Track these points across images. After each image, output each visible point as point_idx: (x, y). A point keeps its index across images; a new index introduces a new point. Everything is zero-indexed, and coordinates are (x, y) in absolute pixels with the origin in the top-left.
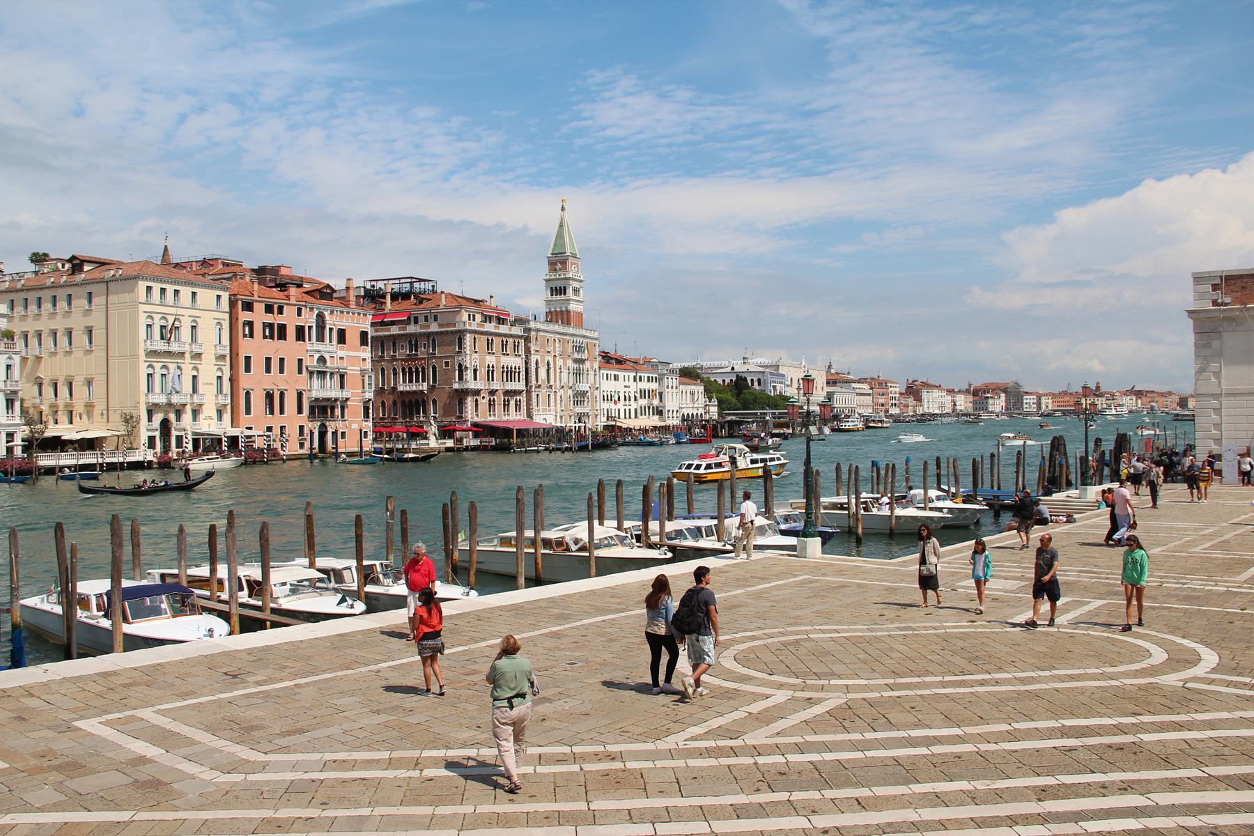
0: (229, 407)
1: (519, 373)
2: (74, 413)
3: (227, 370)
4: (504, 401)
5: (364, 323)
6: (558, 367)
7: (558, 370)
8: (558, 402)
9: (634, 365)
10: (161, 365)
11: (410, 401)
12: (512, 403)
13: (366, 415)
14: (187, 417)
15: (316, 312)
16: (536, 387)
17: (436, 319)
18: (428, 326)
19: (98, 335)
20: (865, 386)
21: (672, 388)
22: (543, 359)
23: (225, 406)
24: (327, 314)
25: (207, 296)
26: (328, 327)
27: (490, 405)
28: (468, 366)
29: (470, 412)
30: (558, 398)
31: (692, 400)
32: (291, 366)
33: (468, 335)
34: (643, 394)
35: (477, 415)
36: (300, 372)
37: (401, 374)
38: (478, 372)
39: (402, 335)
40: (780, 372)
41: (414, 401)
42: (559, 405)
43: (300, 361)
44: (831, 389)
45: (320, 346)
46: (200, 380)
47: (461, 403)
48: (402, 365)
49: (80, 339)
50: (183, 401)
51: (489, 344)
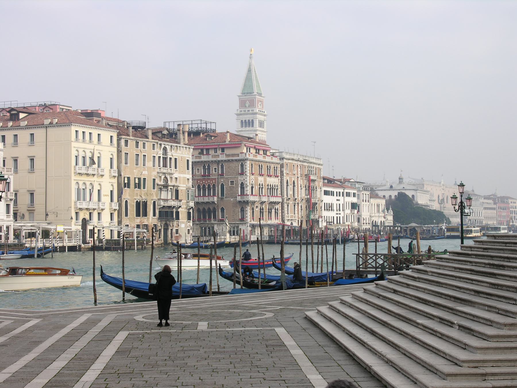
0: (116, 212)
1: (277, 189)
2: (18, 214)
3: (116, 186)
5: (188, 154)
6: (299, 185)
7: (300, 188)
8: (300, 210)
9: (342, 183)
10: (82, 182)
11: (204, 209)
12: (273, 211)
13: (189, 218)
15: (163, 146)
16: (287, 200)
18: (218, 156)
19: (39, 164)
20: (491, 201)
21: (366, 201)
23: (115, 210)
25: (106, 135)
26: (169, 157)
27: (260, 212)
28: (248, 184)
29: (249, 217)
30: (300, 208)
33: (248, 162)
35: (253, 219)
36: (154, 188)
38: (254, 189)
39: (198, 162)
40: (425, 189)
41: (206, 208)
42: (300, 213)
43: (154, 180)
45: (164, 170)
46: (103, 193)
47: (243, 210)
48: (197, 183)
49: (24, 164)
50: (94, 207)
51: (261, 167)
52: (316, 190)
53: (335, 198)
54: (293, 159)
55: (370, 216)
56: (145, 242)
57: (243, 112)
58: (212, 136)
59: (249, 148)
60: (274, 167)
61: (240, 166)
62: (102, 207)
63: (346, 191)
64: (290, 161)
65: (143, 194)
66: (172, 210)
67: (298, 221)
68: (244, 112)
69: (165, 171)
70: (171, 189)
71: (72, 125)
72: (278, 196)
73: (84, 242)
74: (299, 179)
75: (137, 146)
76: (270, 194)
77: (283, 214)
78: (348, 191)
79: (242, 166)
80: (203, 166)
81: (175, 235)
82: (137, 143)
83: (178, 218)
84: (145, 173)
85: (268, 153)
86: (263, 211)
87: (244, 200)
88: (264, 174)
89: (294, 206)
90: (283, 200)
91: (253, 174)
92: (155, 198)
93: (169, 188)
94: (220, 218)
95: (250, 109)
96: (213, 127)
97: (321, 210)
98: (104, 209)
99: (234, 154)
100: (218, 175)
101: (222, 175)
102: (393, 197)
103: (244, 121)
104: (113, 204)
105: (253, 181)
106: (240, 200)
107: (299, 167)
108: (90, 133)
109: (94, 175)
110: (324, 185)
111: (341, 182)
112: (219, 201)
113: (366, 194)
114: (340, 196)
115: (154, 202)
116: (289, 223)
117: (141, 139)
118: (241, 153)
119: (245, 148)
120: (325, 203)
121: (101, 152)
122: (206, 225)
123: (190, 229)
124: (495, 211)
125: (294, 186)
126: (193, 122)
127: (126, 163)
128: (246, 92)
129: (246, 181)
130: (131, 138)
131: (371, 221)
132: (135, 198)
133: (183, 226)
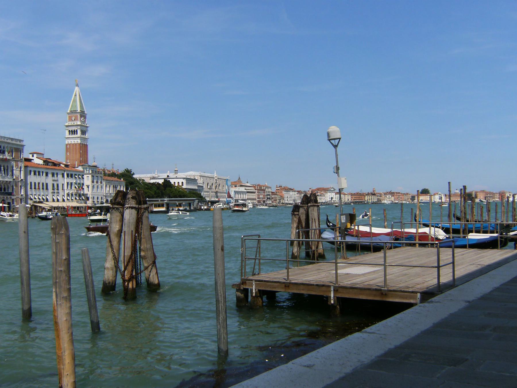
57: (70, 124)
68: (71, 124)
95: (75, 122)
128: (72, 110)
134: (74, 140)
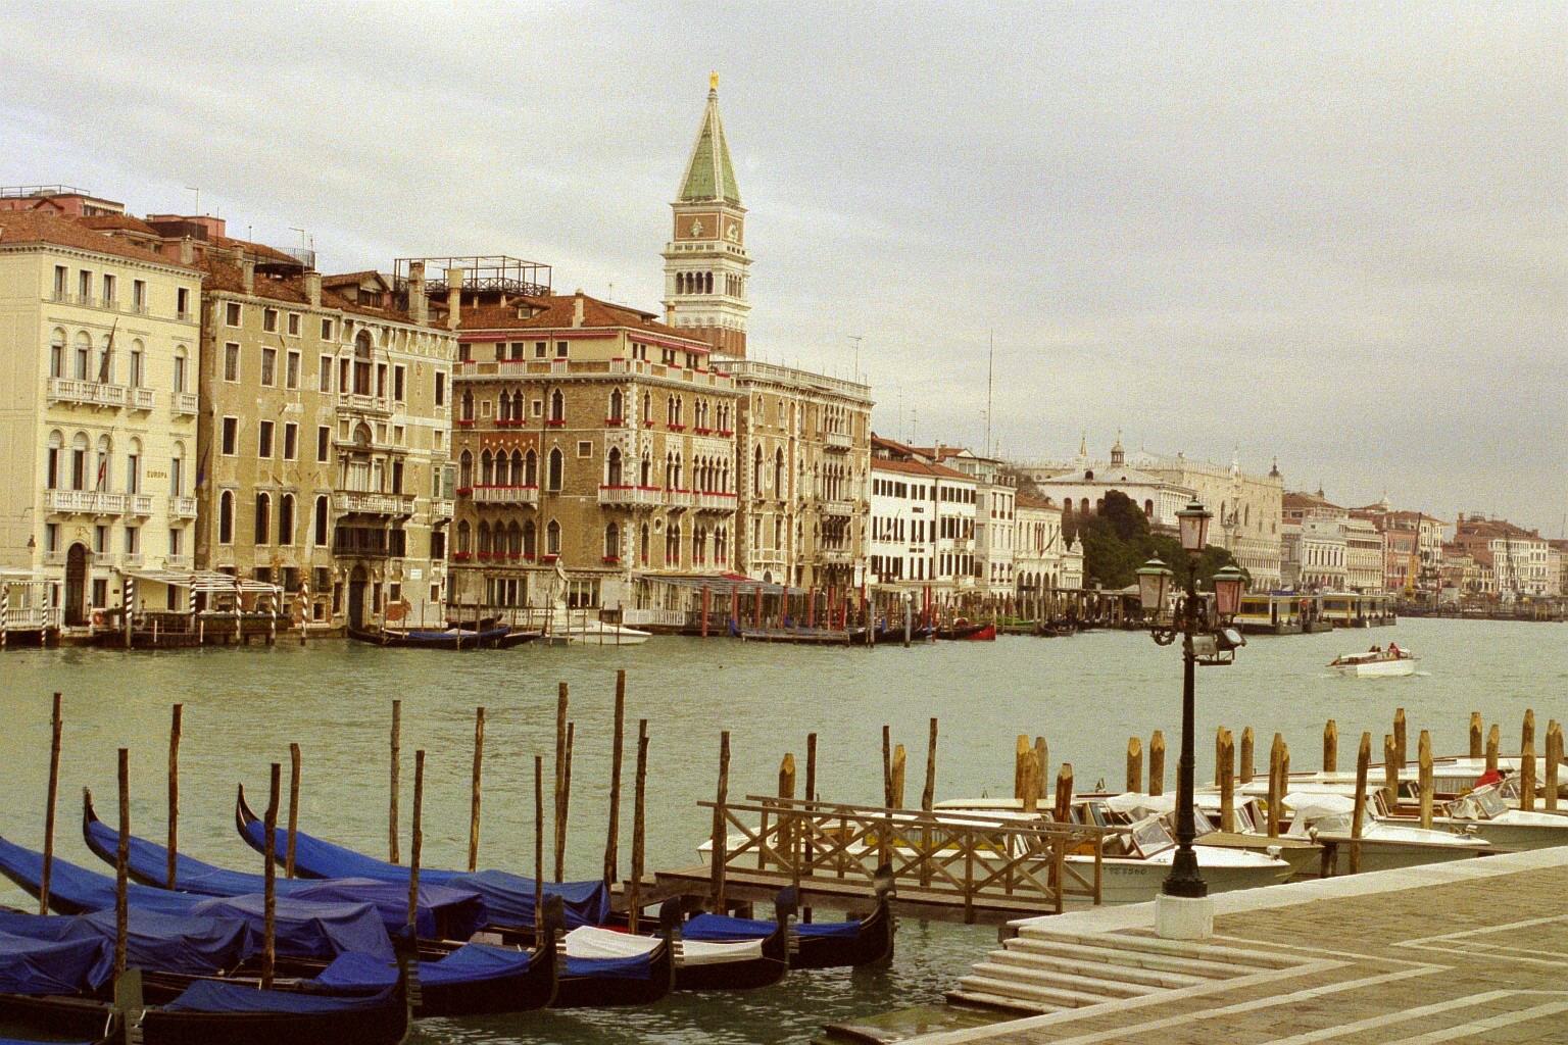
0: (191, 527)
1: (725, 473)
3: (191, 444)
4: (696, 531)
6: (797, 463)
7: (797, 471)
8: (795, 537)
9: (933, 461)
11: (499, 524)
12: (710, 536)
14: (117, 537)
15: (357, 328)
16: (755, 505)
17: (562, 350)
18: (547, 366)
20: (1368, 525)
22: (769, 441)
23: (186, 521)
24: (376, 335)
25: (162, 287)
26: (376, 362)
27: (669, 539)
28: (633, 455)
29: (632, 554)
30: (795, 529)
31: (1039, 544)
32: (306, 443)
33: (635, 389)
34: (950, 527)
35: (645, 558)
36: (322, 457)
37: (480, 466)
38: (650, 469)
39: (487, 383)
41: (506, 523)
42: (795, 546)
43: (324, 432)
44: (1292, 529)
46: (144, 464)
47: (613, 532)
50: (112, 510)
51: (674, 405)
52: (850, 480)
53: (908, 503)
54: (778, 385)
55: (1014, 560)
56: (273, 625)
57: (683, 251)
58: (532, 307)
59: (640, 346)
60: (719, 407)
61: (610, 398)
62: (142, 511)
63: (942, 483)
64: (770, 391)
65: (285, 475)
66: (381, 527)
67: (789, 568)
69: (362, 405)
70: (379, 460)
71: (43, 248)
72: (727, 491)
73: (74, 616)
74: (797, 444)
75: (270, 326)
76: (702, 486)
77: (743, 547)
78: (948, 484)
79: (617, 397)
80: (502, 397)
81: (389, 603)
82: (270, 315)
83: (399, 549)
84: (294, 409)
85: (702, 364)
86: (678, 538)
87: (619, 501)
88: (684, 427)
89: (778, 523)
90: (742, 508)
91: (649, 425)
92: (324, 486)
93: (374, 457)
94: (546, 554)
95: (705, 243)
96: (542, 281)
97: (863, 539)
98: (148, 517)
99: (595, 363)
100: (546, 423)
101: (557, 422)
102: (1093, 505)
103: (684, 276)
104: (179, 503)
105: (650, 447)
106: (607, 501)
107: (797, 408)
108: (108, 278)
109: (115, 409)
110: (877, 463)
111: (930, 458)
112: (545, 502)
113: (1003, 495)
114: (922, 497)
115: (322, 503)
116: (757, 576)
117: (284, 304)
118: (614, 360)
119: (629, 347)
120: (875, 519)
121: (143, 338)
122: (504, 573)
123: (440, 584)
124: (1379, 553)
125: (779, 465)
126: (481, 263)
127: (231, 376)
128: (694, 193)
129: (627, 445)
130: (250, 297)
131: (1017, 574)
132: (257, 484)
133: (416, 574)
134: (696, 315)
